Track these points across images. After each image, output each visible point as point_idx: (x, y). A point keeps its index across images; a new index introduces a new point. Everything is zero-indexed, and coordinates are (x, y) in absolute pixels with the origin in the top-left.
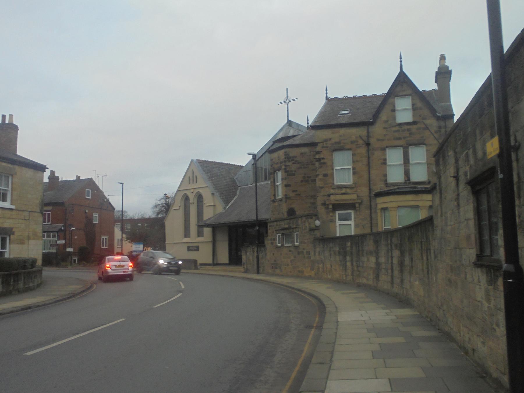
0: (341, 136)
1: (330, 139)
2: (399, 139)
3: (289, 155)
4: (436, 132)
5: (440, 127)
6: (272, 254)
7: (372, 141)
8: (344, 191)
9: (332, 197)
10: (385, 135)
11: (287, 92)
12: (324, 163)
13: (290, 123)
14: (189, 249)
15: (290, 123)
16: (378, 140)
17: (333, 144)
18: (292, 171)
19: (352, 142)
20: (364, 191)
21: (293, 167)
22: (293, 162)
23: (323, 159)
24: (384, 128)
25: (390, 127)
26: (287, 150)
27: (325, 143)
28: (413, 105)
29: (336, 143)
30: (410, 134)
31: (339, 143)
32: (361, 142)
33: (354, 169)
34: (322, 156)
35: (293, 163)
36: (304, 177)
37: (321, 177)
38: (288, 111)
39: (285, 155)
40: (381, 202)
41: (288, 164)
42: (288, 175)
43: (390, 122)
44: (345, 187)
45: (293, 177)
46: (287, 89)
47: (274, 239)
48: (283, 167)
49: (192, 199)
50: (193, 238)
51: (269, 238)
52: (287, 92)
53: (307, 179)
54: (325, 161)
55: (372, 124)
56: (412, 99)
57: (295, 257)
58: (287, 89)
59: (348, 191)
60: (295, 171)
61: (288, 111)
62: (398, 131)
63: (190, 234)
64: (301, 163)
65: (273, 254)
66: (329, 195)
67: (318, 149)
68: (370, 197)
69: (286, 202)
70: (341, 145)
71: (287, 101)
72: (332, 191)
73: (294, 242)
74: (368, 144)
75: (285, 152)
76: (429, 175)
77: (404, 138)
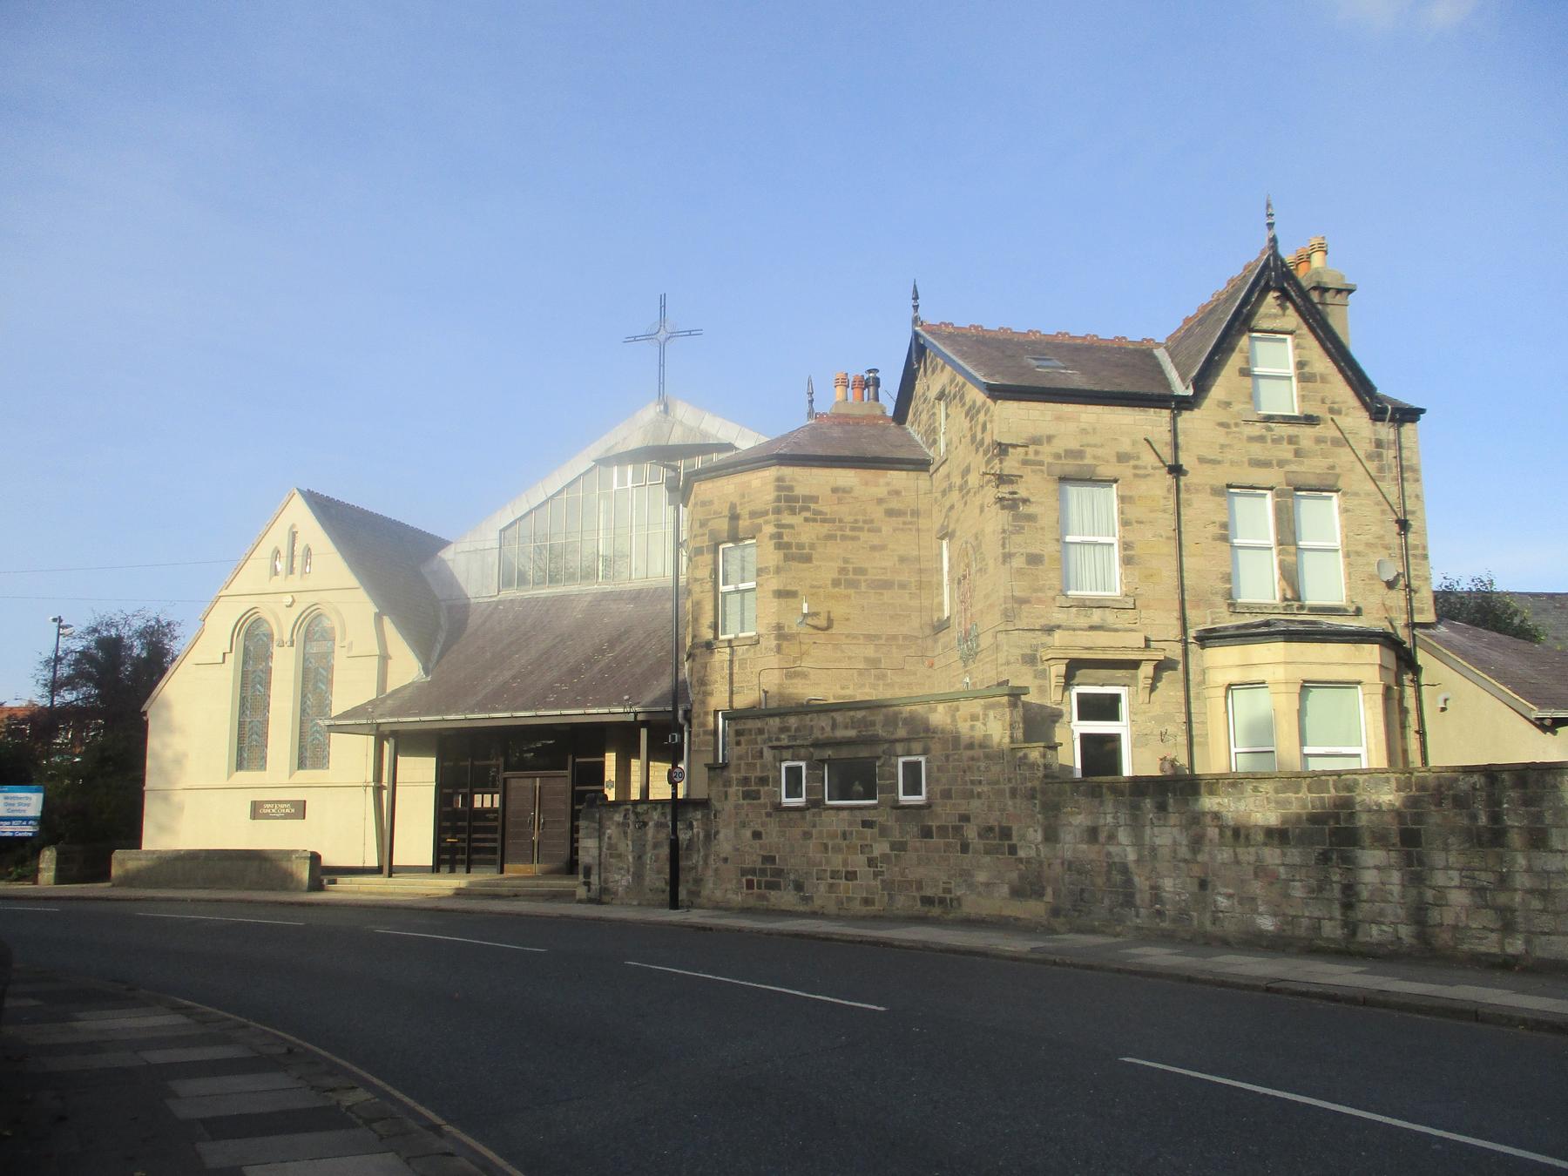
0: (1084, 431)
1: (1050, 438)
2: (1266, 464)
3: (791, 488)
4: (1370, 457)
5: (1379, 444)
6: (748, 833)
7: (1184, 460)
8: (1096, 617)
9: (1058, 638)
10: (1222, 446)
12: (1031, 518)
14: (257, 811)
16: (1202, 460)
17: (1058, 456)
18: (800, 546)
19: (1122, 458)
20: (1164, 626)
21: (806, 533)
22: (808, 514)
23: (1025, 501)
24: (1222, 425)
25: (1237, 425)
26: (787, 471)
27: (1032, 449)
28: (1301, 365)
29: (1070, 454)
30: (1297, 453)
31: (1078, 454)
32: (1149, 458)
33: (1126, 546)
34: (1023, 493)
35: (806, 520)
36: (842, 570)
37: (1018, 562)
39: (779, 488)
40: (1223, 662)
41: (787, 519)
42: (787, 558)
43: (1236, 407)
44: (1101, 605)
45: (805, 565)
47: (763, 781)
48: (769, 529)
53: (851, 576)
54: (1030, 509)
55: (1185, 404)
56: (1297, 347)
57: (899, 847)
59: (1110, 617)
60: (812, 546)
62: (1261, 439)
63: (264, 758)
64: (833, 521)
65: (757, 835)
66: (1050, 630)
67: (1011, 465)
68: (1185, 643)
69: (779, 649)
70: (1087, 461)
71: (662, 335)
72: (1058, 617)
74: (1176, 470)
75: (779, 479)
76: (1350, 588)
77: (1281, 463)
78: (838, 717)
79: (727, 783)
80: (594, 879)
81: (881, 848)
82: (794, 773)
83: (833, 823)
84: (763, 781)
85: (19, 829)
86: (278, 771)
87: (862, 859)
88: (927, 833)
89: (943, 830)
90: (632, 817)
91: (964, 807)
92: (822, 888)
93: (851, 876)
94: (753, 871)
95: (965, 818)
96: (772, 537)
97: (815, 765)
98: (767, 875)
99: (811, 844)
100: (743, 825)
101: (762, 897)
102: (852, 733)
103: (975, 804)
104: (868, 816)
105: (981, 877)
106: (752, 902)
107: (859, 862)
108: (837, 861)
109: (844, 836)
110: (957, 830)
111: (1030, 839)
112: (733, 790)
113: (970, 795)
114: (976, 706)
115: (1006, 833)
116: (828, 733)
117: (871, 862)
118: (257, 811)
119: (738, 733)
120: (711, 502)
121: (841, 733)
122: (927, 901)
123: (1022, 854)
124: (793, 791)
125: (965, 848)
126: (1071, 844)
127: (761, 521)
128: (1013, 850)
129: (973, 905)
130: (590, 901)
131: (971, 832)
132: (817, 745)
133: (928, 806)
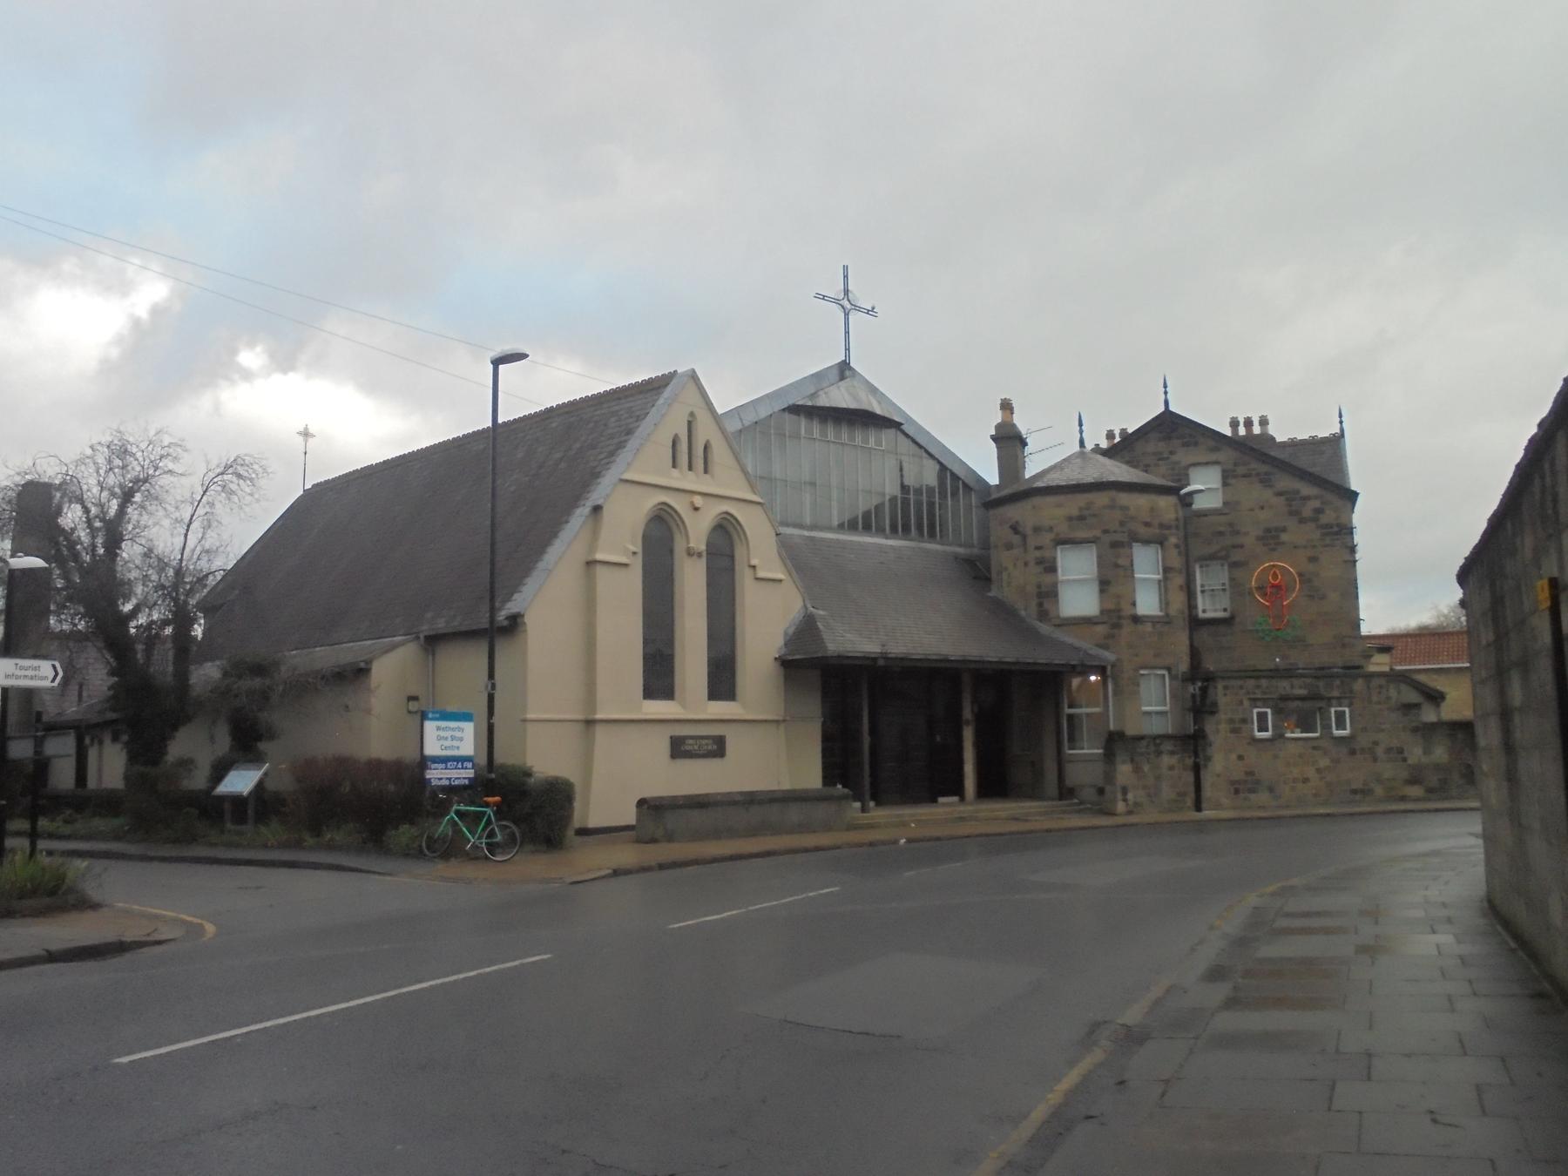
6: (1234, 756)
13: (844, 369)
14: (679, 749)
15: (844, 369)
38: (847, 332)
46: (845, 268)
47: (1244, 721)
50: (692, 702)
51: (1222, 716)
57: (1336, 761)
58: (845, 268)
61: (847, 332)
65: (1240, 758)
71: (845, 303)
78: (1296, 682)
80: (1130, 796)
81: (1324, 762)
82: (1262, 717)
84: (1244, 721)
85: (454, 774)
86: (692, 702)
88: (1353, 752)
89: (1363, 750)
90: (1152, 748)
93: (1306, 780)
94: (1238, 782)
95: (1376, 743)
96: (1177, 546)
97: (1278, 712)
104: (1315, 744)
107: (1311, 772)
109: (1300, 756)
112: (1223, 726)
114: (1382, 681)
115: (1400, 751)
117: (1319, 771)
118: (679, 749)
119: (1226, 688)
122: (1354, 792)
124: (1263, 728)
125: (1375, 760)
128: (1405, 760)
130: (1130, 813)
131: (1380, 751)
133: (1351, 738)
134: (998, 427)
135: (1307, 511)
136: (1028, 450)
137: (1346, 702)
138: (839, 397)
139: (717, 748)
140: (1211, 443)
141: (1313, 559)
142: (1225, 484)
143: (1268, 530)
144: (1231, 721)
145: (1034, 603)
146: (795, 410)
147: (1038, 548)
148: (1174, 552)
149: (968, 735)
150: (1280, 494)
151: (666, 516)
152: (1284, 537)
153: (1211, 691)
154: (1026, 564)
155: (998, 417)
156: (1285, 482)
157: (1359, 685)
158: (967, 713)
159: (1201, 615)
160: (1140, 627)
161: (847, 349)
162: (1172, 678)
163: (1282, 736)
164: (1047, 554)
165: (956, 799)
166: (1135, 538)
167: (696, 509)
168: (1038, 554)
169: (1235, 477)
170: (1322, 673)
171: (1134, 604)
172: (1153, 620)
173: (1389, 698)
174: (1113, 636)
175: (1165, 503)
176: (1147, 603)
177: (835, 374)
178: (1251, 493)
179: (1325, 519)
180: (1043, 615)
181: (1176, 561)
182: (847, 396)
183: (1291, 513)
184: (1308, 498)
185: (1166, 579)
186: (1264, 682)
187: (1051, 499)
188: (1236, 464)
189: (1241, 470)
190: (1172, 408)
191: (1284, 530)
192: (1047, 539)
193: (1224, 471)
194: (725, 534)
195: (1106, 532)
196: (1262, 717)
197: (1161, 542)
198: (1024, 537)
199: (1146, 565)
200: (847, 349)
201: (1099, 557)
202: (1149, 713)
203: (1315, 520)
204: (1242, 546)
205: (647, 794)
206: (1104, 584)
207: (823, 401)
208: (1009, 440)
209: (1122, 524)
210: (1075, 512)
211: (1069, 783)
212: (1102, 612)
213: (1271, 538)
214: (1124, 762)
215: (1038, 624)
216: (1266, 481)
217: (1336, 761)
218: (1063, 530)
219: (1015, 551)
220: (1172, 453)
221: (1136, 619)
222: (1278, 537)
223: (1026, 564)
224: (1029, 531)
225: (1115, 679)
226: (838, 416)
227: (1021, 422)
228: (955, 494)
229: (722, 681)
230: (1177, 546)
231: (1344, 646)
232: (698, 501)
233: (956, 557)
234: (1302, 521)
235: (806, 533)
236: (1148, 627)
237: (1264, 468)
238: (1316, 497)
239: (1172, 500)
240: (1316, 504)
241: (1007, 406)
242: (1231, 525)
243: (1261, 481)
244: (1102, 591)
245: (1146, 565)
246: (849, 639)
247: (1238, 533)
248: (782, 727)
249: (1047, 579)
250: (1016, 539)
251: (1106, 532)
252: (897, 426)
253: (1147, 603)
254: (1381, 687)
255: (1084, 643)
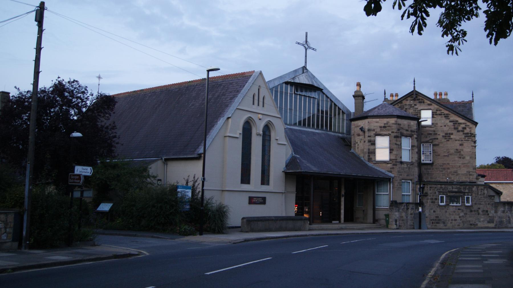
6: (432, 211)
11: (306, 36)
14: (252, 201)
47: (436, 199)
49: (258, 129)
52: (306, 36)
57: (466, 214)
65: (434, 212)
73: (464, 202)
78: (454, 186)
79: (428, 199)
80: (398, 223)
81: (462, 214)
83: (451, 209)
84: (436, 199)
87: (458, 216)
88: (471, 211)
89: (475, 211)
90: (406, 207)
91: (479, 206)
92: (449, 223)
93: (455, 220)
94: (433, 220)
95: (479, 208)
96: (416, 138)
98: (437, 221)
99: (448, 213)
100: (431, 209)
101: (435, 226)
102: (456, 190)
103: (481, 206)
104: (459, 208)
105: (482, 220)
106: (433, 227)
107: (457, 217)
108: (453, 217)
109: (454, 212)
110: (478, 211)
111: (492, 213)
112: (429, 201)
113: (480, 204)
114: (482, 188)
115: (487, 211)
116: (451, 190)
117: (460, 217)
118: (252, 201)
119: (430, 188)
120: (400, 125)
121: (454, 190)
122: (471, 225)
123: (490, 215)
124: (442, 201)
125: (479, 214)
126: (500, 213)
127: (413, 133)
128: (488, 214)
129: (480, 224)
130: (397, 229)
131: (480, 211)
132: (450, 192)
133: (471, 206)
134: (355, 92)
135: (460, 128)
136: (365, 100)
137: (470, 194)
138: (303, 79)
139: (263, 201)
140: (429, 102)
141: (461, 145)
142: (433, 117)
143: (446, 134)
144: (432, 199)
145: (367, 155)
146: (287, 83)
147: (369, 136)
148: (415, 140)
149: (343, 199)
150: (450, 122)
151: (250, 122)
152: (452, 137)
153: (426, 188)
154: (364, 142)
155: (356, 88)
156: (454, 117)
157: (474, 189)
158: (343, 193)
159: (422, 162)
160: (403, 166)
161: (306, 62)
162: (413, 183)
163: (448, 205)
164: (372, 139)
165: (338, 222)
166: (402, 135)
167: (260, 119)
168: (369, 138)
169: (436, 115)
170: (462, 183)
171: (401, 157)
172: (407, 163)
173: (484, 193)
174: (393, 168)
175: (413, 123)
176: (406, 157)
177: (301, 72)
178: (441, 121)
179: (466, 131)
180: (370, 160)
181: (416, 144)
182: (305, 79)
183: (455, 129)
184: (461, 124)
185: (412, 149)
186: (443, 186)
187: (374, 120)
188: (437, 110)
189: (438, 112)
190: (416, 89)
191: (452, 134)
192: (372, 133)
193: (433, 112)
194: (267, 128)
195: (392, 132)
196: (442, 198)
197: (411, 136)
198: (364, 132)
199: (406, 143)
200: (306, 62)
201: (390, 141)
202: (420, 199)
203: (463, 131)
204: (437, 139)
205: (245, 216)
206: (391, 151)
207: (297, 81)
208: (359, 97)
209: (398, 130)
210: (383, 125)
211: (376, 218)
212: (390, 160)
213: (447, 136)
214: (396, 212)
215: (367, 163)
216: (447, 117)
217: (466, 214)
218: (378, 130)
219: (361, 137)
220: (415, 105)
221: (402, 163)
222: (450, 136)
223: (364, 142)
224: (366, 130)
225: (393, 183)
226: (302, 87)
227: (364, 90)
228: (339, 114)
229: (265, 180)
230: (416, 138)
231: (470, 175)
232: (260, 116)
233: (339, 137)
234: (458, 131)
235: (289, 127)
236: (405, 166)
237: (446, 112)
238: (463, 124)
239: (416, 122)
240: (463, 126)
241: (359, 85)
242: (434, 131)
243: (445, 117)
244: (390, 153)
245: (406, 143)
246: (309, 167)
247: (436, 134)
248: (284, 195)
249: (372, 147)
250: (361, 133)
251: (392, 132)
252: (321, 90)
253: (406, 157)
254: (482, 189)
255: (383, 170)
